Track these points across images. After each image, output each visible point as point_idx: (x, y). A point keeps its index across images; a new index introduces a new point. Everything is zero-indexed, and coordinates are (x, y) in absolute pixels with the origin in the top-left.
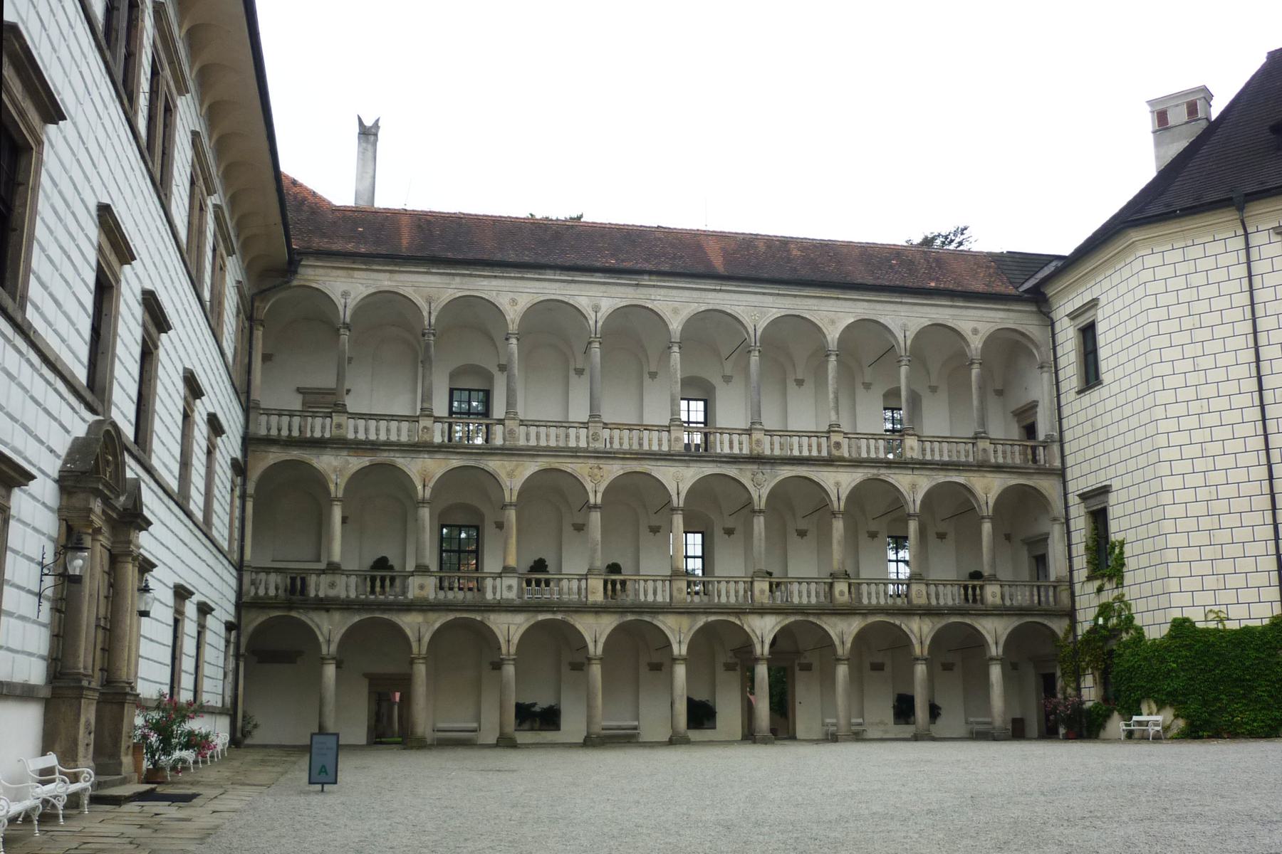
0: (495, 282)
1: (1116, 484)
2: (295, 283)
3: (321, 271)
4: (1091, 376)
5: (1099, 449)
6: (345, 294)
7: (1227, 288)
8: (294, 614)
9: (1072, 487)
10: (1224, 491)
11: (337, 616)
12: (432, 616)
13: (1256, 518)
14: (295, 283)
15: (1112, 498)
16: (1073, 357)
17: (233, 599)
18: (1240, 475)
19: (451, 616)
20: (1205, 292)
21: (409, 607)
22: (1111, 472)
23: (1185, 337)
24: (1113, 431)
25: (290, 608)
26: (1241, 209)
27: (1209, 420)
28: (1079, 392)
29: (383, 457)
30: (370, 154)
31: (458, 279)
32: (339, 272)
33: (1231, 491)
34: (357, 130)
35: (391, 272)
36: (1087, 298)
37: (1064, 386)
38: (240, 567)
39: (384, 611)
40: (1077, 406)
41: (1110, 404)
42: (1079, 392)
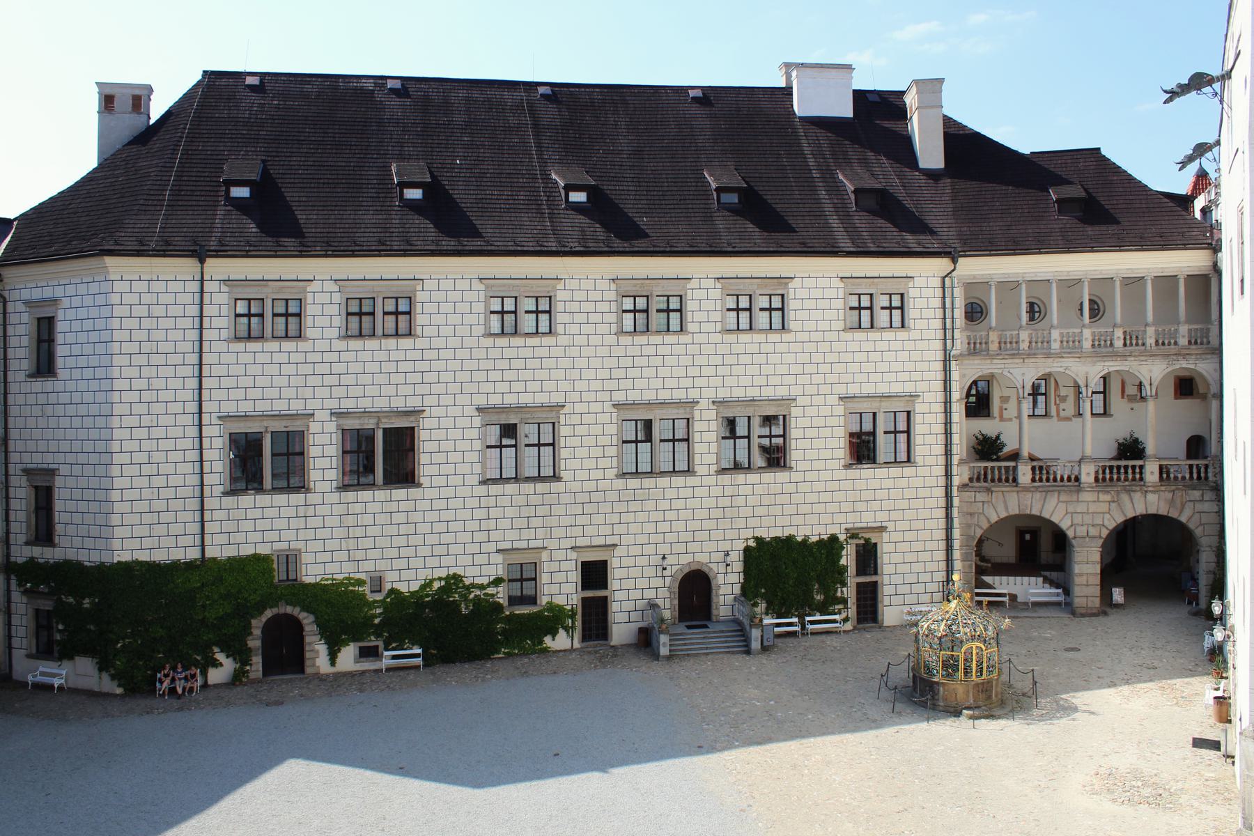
1: (64, 470)
4: (45, 366)
5: (48, 434)
7: (182, 323)
9: (14, 458)
10: (165, 493)
13: (188, 516)
15: (58, 481)
16: (25, 341)
18: (178, 480)
20: (164, 323)
22: (60, 458)
23: (143, 360)
24: (65, 422)
26: (202, 262)
27: (156, 433)
28: (30, 376)
33: (170, 493)
36: (48, 293)
37: (13, 365)
40: (26, 387)
41: (64, 398)
42: (30, 376)
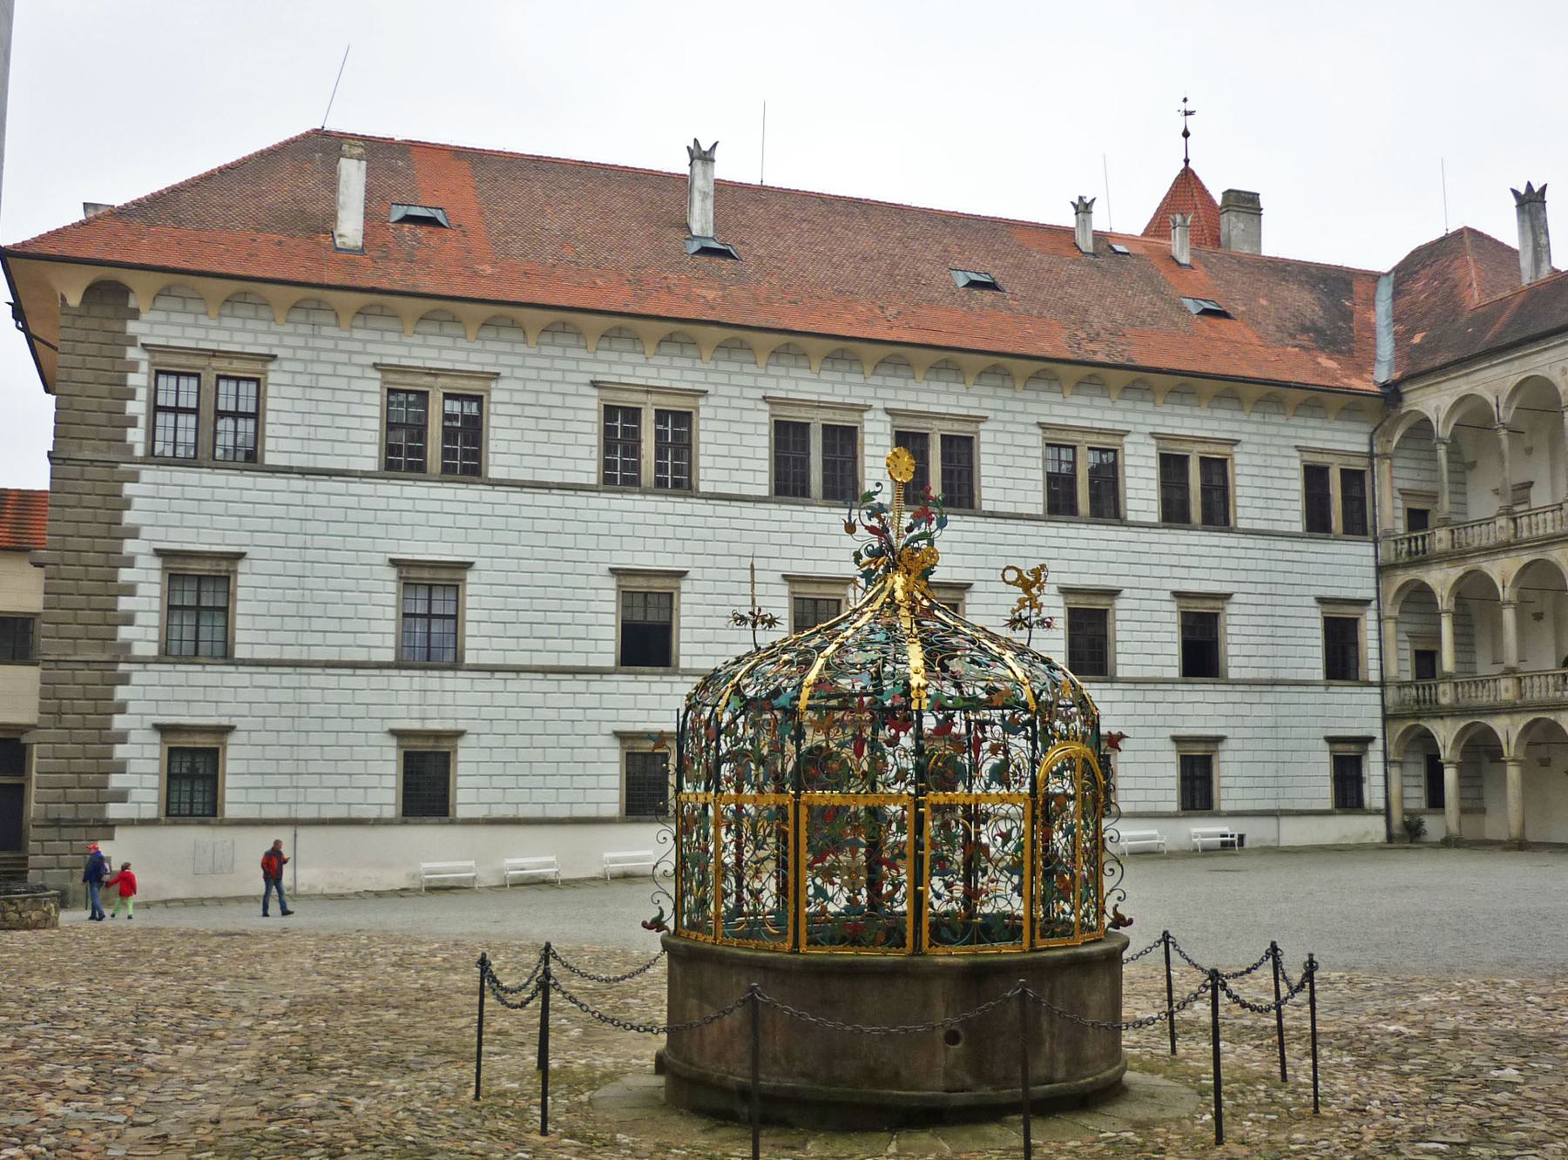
0: (1547, 355)
2: (1403, 411)
3: (1419, 393)
6: (1437, 409)
8: (1421, 723)
11: (1448, 722)
12: (1517, 717)
14: (1403, 411)
17: (1378, 711)
19: (1531, 717)
21: (1495, 711)
25: (1419, 718)
29: (1472, 564)
30: (1528, 225)
31: (1517, 363)
32: (1432, 389)
34: (1514, 202)
35: (1467, 375)
38: (1382, 684)
39: (1481, 715)
